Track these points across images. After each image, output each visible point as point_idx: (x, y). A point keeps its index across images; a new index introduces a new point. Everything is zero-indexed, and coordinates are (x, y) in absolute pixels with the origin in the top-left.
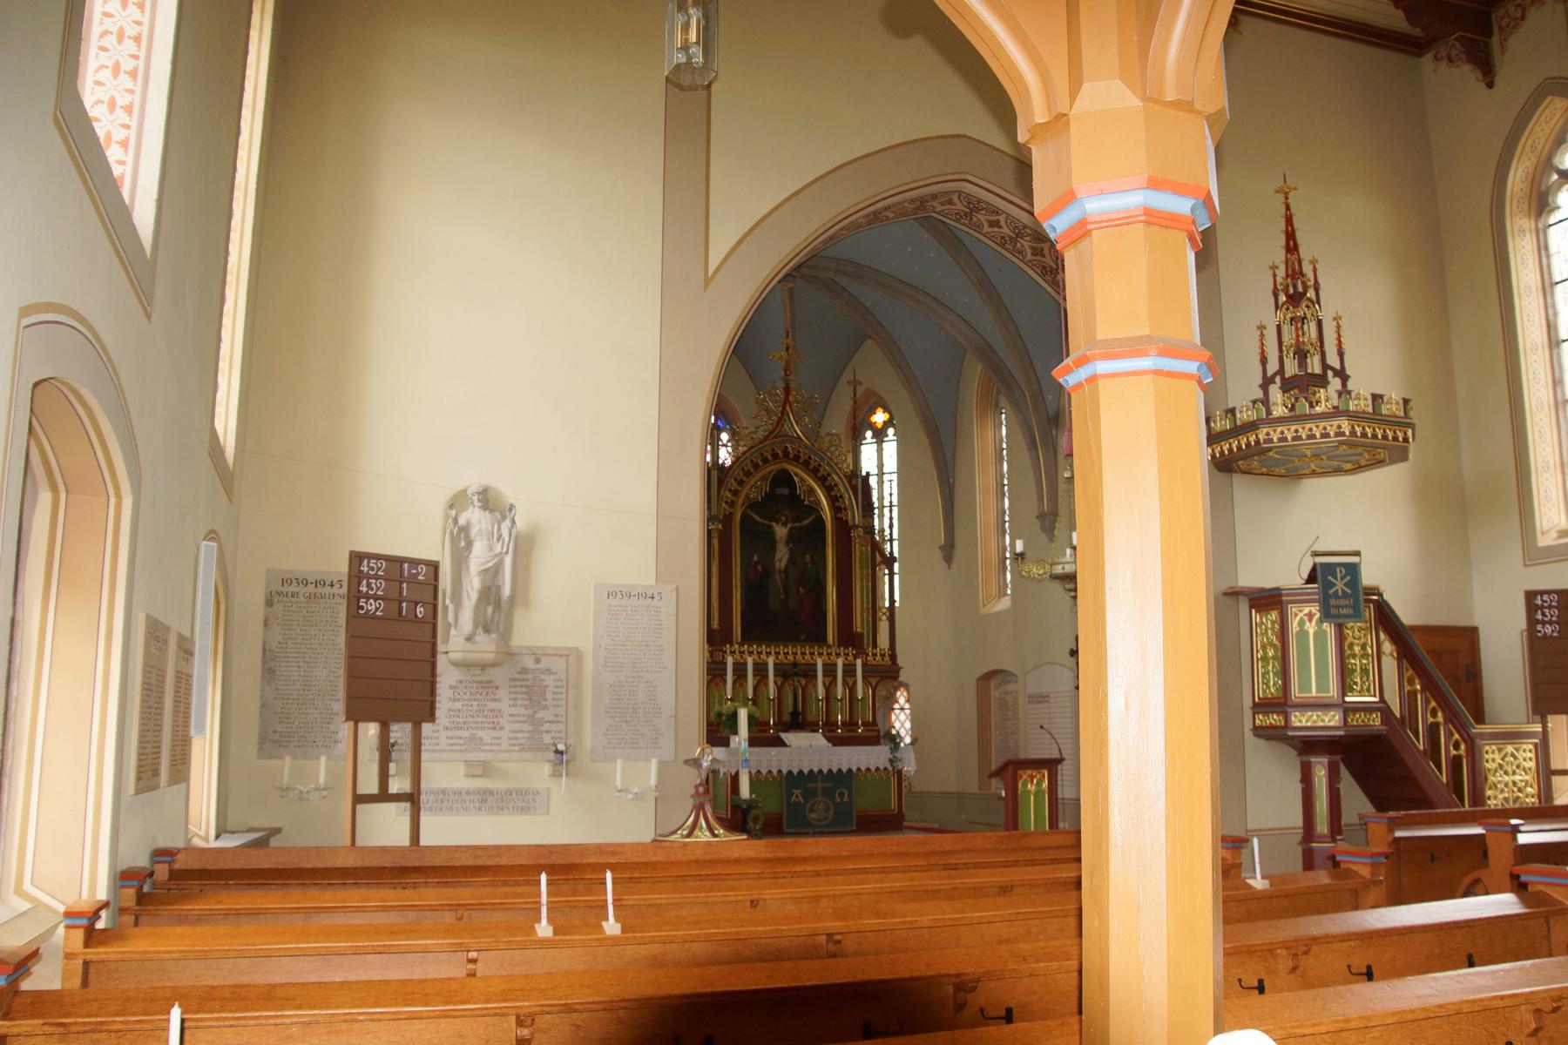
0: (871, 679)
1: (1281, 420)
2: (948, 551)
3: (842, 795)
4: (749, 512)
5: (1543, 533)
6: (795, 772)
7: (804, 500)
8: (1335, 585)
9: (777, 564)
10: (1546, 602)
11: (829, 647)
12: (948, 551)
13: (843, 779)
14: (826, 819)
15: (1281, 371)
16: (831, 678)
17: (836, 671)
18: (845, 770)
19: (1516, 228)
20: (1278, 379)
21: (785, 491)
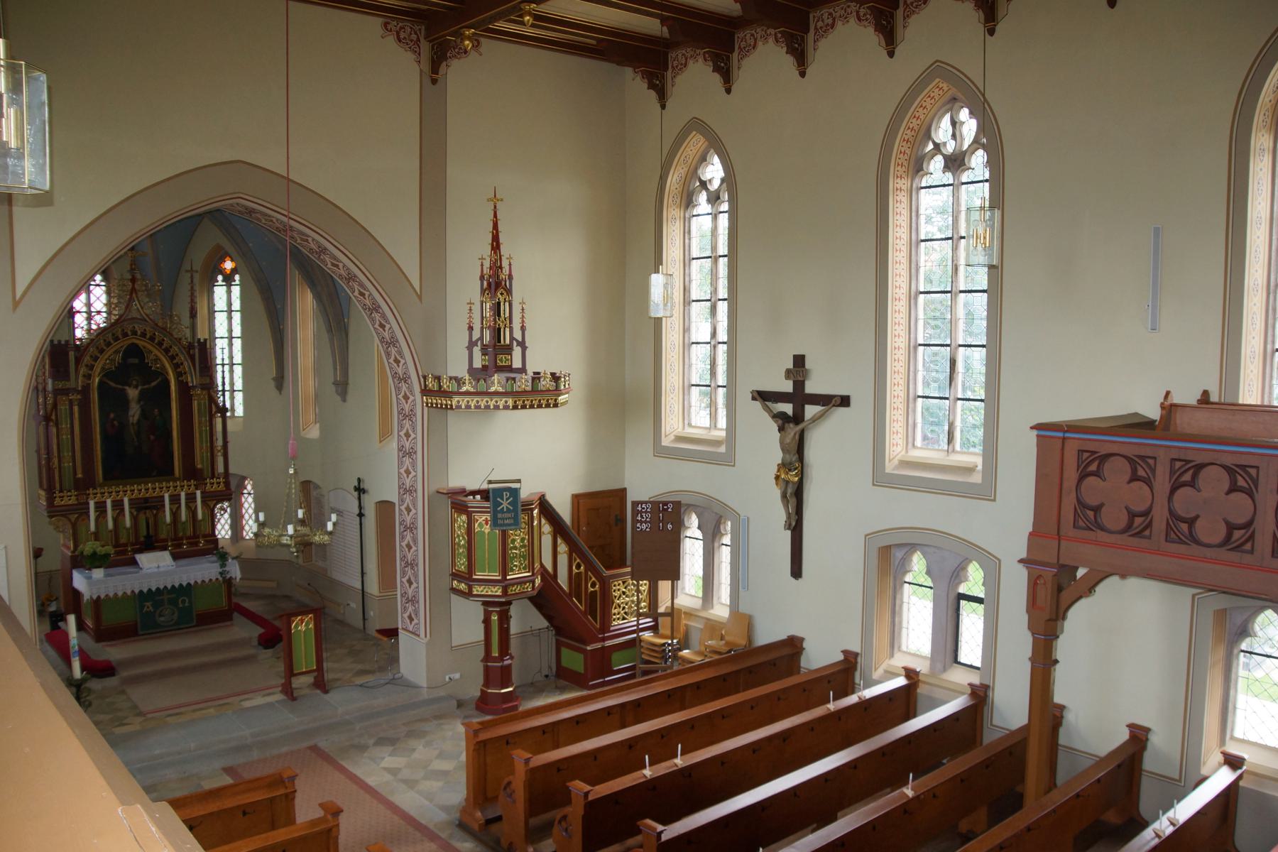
0: (209, 503)
1: (467, 393)
2: (280, 382)
3: (184, 602)
5: (666, 436)
6: (145, 590)
8: (502, 504)
9: (131, 419)
10: (644, 508)
11: (175, 480)
12: (280, 382)
13: (184, 591)
14: (173, 620)
15: (481, 338)
16: (177, 506)
17: (180, 500)
18: (184, 584)
19: (670, 217)
20: (479, 343)
21: (136, 361)
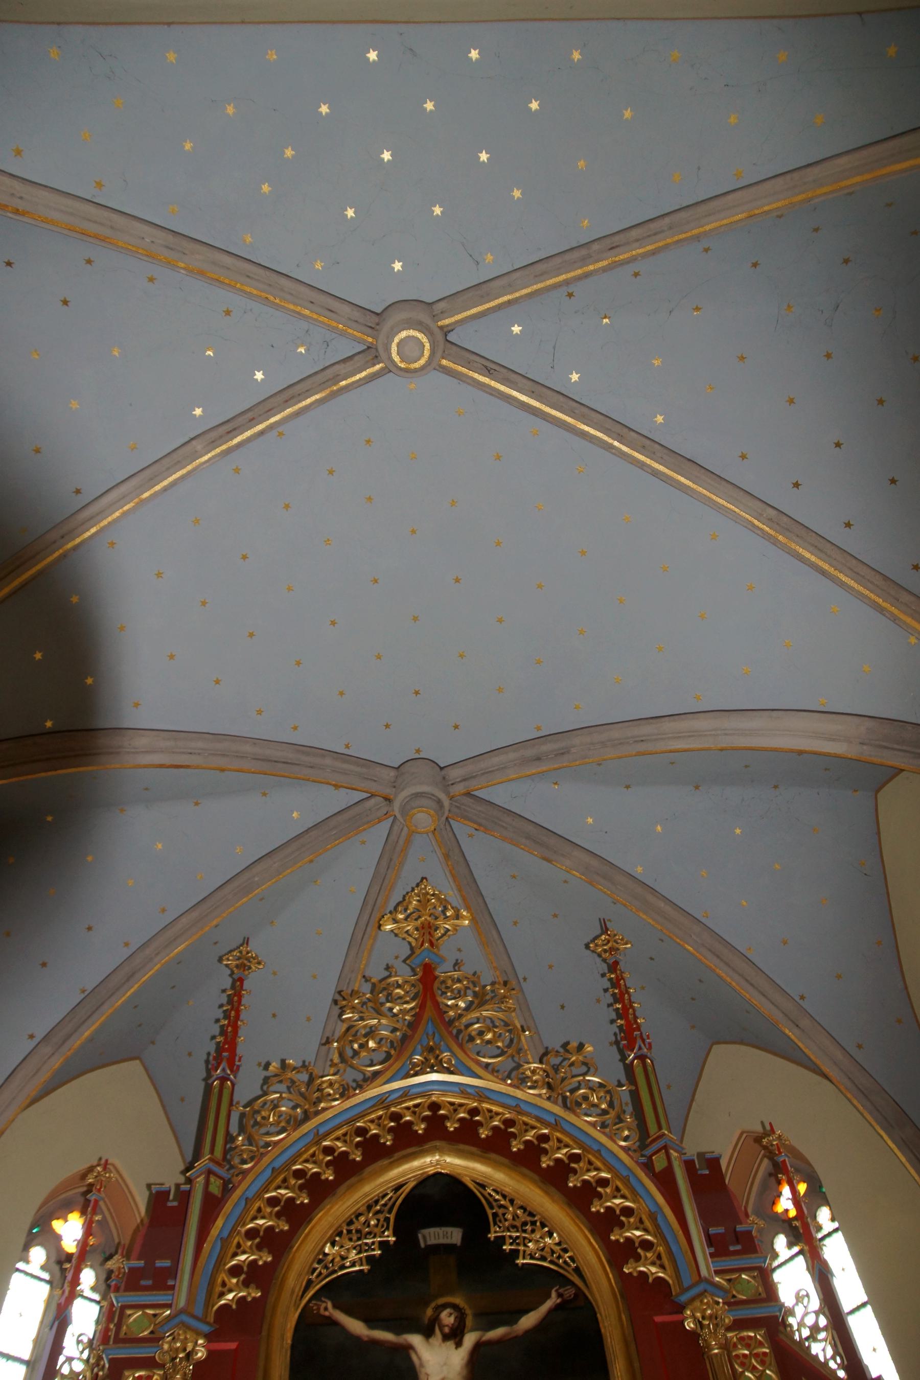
4: (329, 1309)
7: (515, 1253)
21: (454, 1236)
